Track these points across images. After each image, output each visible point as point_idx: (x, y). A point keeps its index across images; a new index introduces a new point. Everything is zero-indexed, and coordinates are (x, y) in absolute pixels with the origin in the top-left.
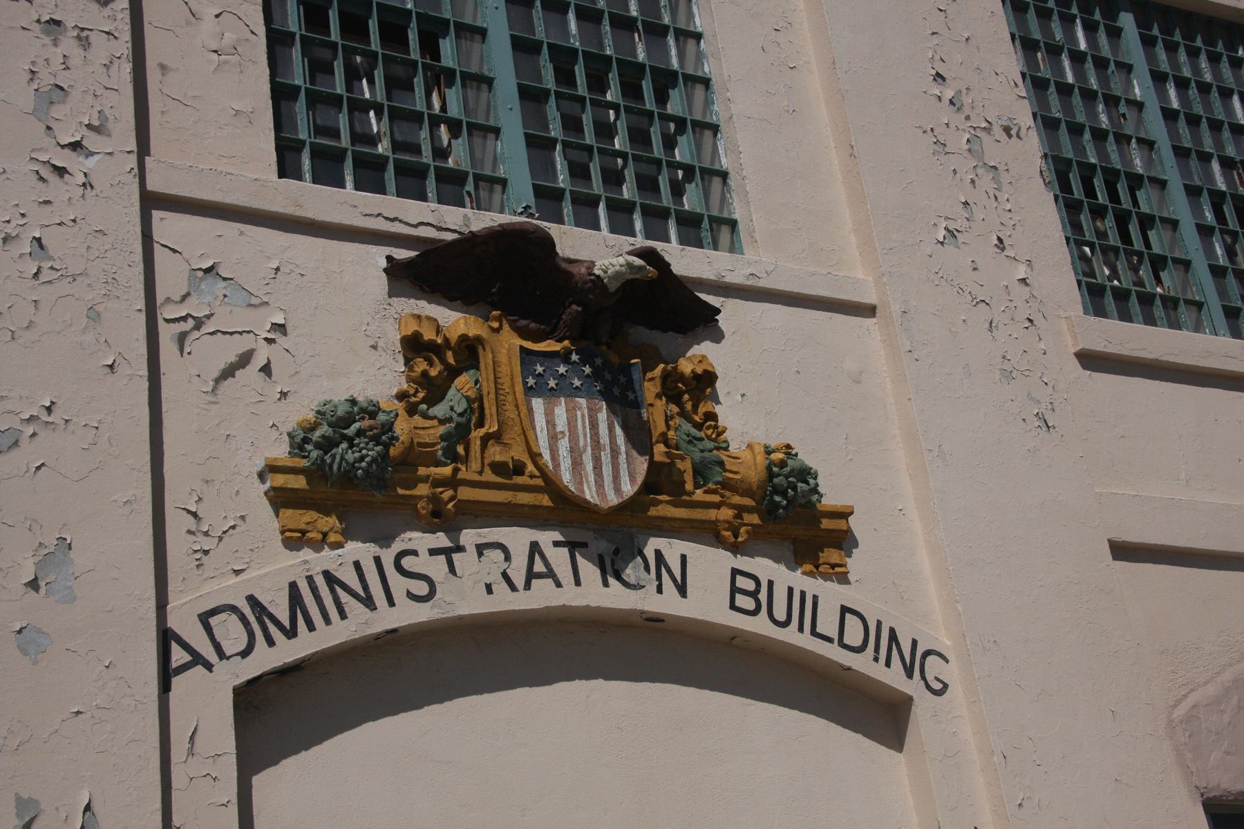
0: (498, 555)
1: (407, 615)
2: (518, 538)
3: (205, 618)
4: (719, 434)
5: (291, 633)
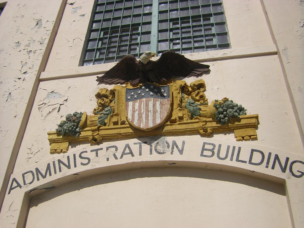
0: (114, 149)
1: (80, 169)
2: (121, 144)
3: (23, 175)
4: (204, 101)
5: (44, 177)
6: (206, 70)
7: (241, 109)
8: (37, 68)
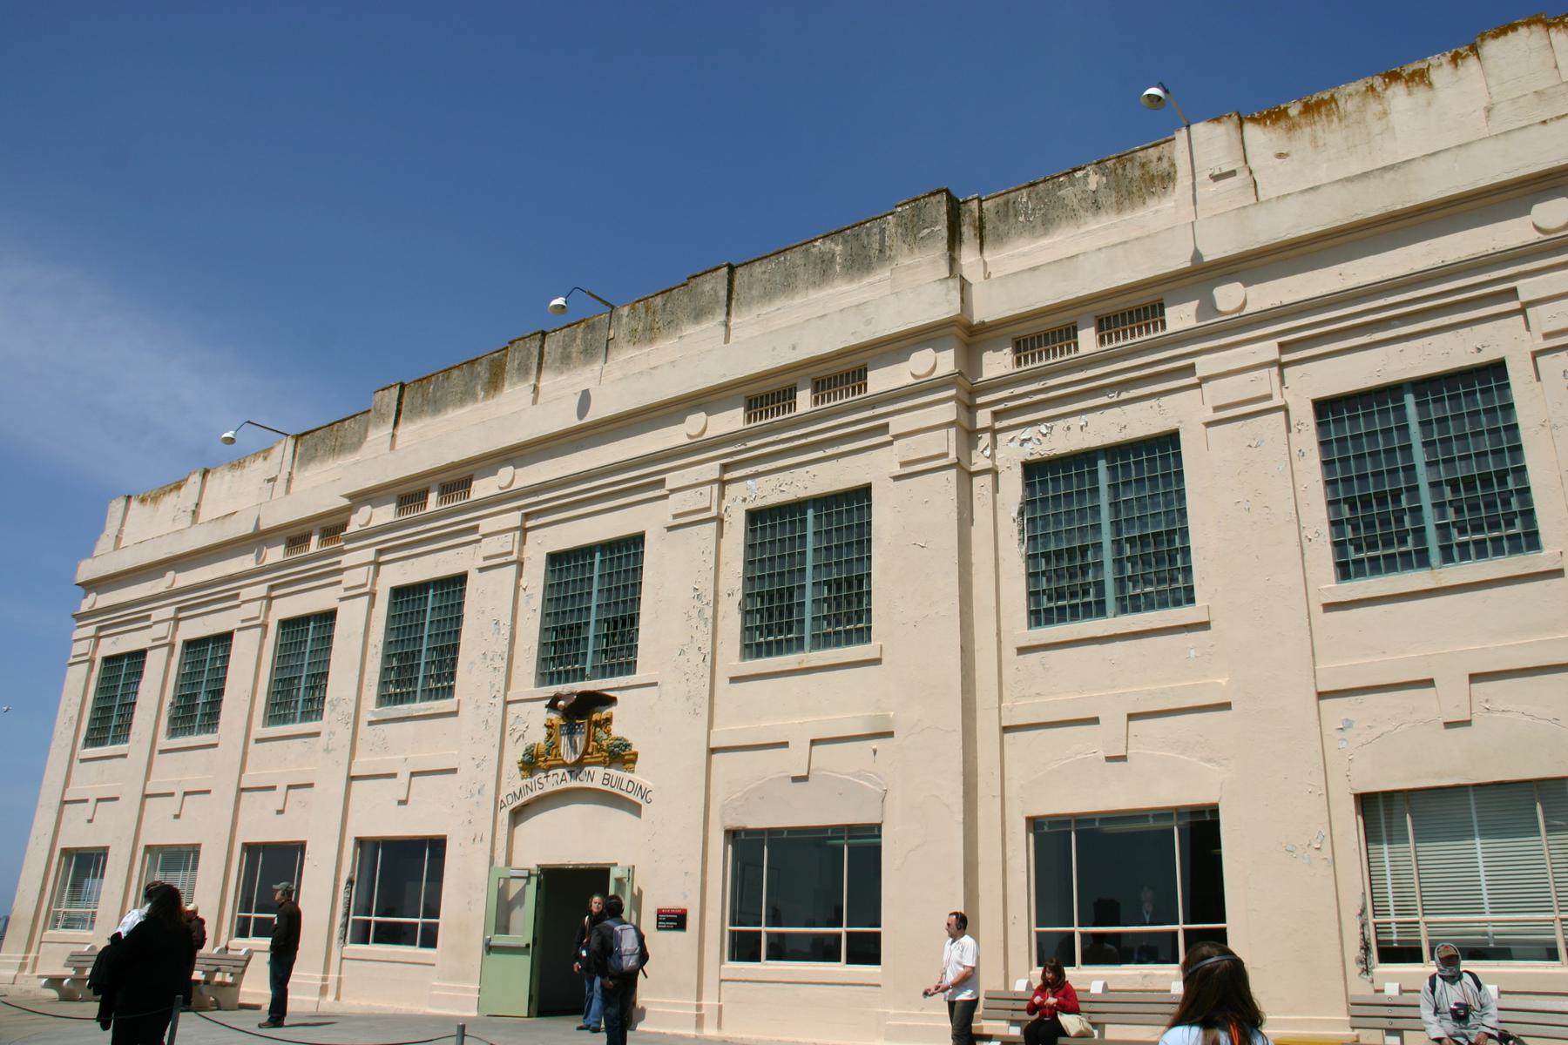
1: (538, 792)
5: (519, 799)
6: (612, 701)
7: (628, 746)
8: (502, 692)
